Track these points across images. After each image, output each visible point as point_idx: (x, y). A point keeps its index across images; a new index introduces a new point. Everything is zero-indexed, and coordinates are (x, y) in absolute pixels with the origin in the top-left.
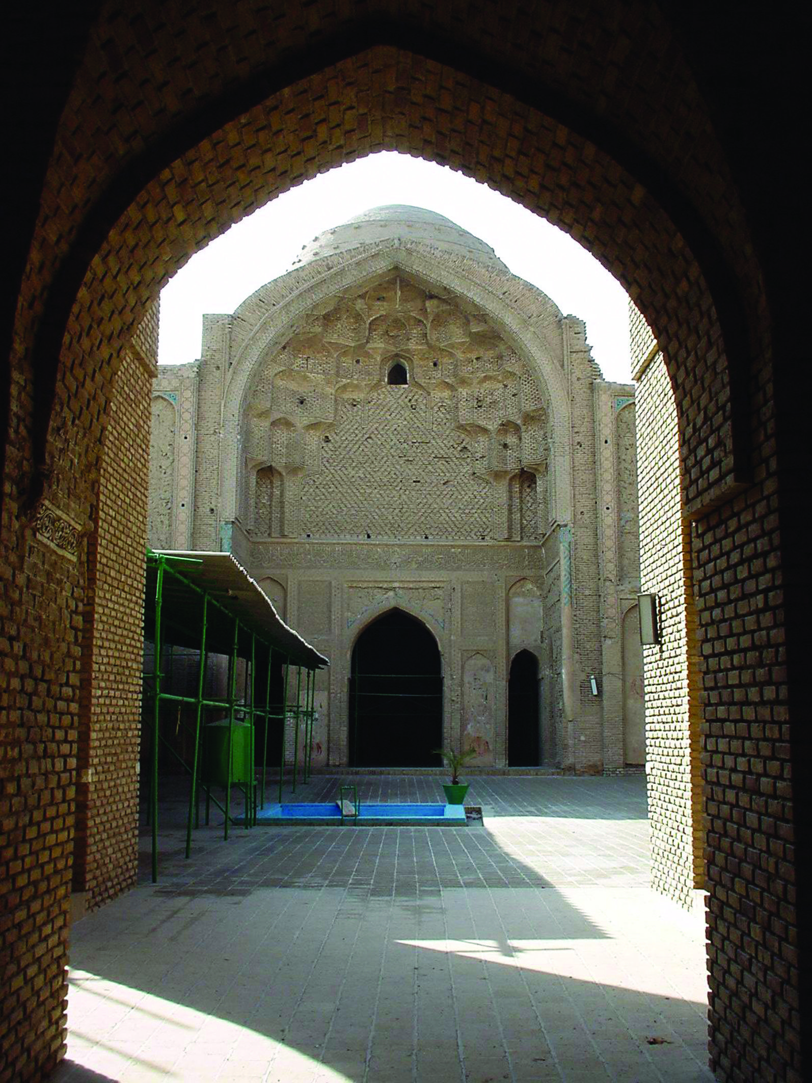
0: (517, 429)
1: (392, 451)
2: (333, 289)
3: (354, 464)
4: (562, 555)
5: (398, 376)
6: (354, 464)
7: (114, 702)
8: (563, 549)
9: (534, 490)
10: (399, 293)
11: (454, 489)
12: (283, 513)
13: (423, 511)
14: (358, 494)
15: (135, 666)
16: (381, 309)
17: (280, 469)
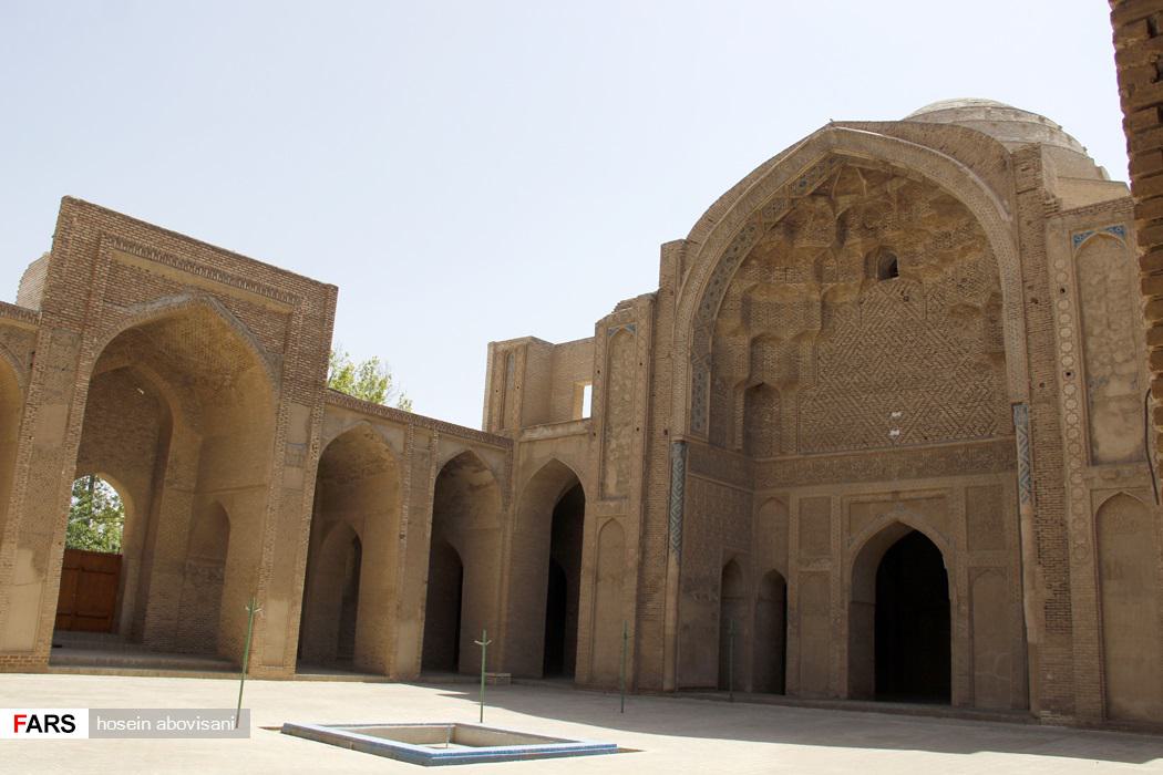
1: (886, 350)
3: (850, 370)
5: (892, 271)
6: (850, 370)
10: (865, 182)
11: (953, 382)
13: (921, 410)
14: (854, 402)
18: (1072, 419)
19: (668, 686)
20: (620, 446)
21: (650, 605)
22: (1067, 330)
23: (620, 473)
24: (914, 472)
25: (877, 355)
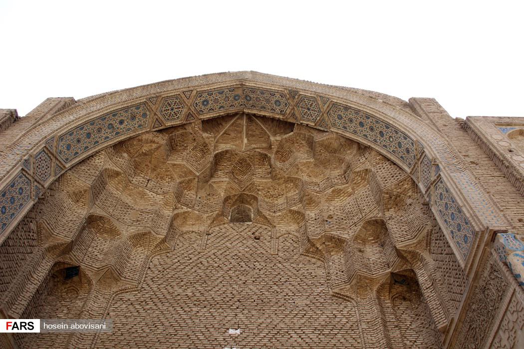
1: (231, 272)
6: (182, 283)
10: (245, 141)
17: (90, 274)
25: (219, 275)
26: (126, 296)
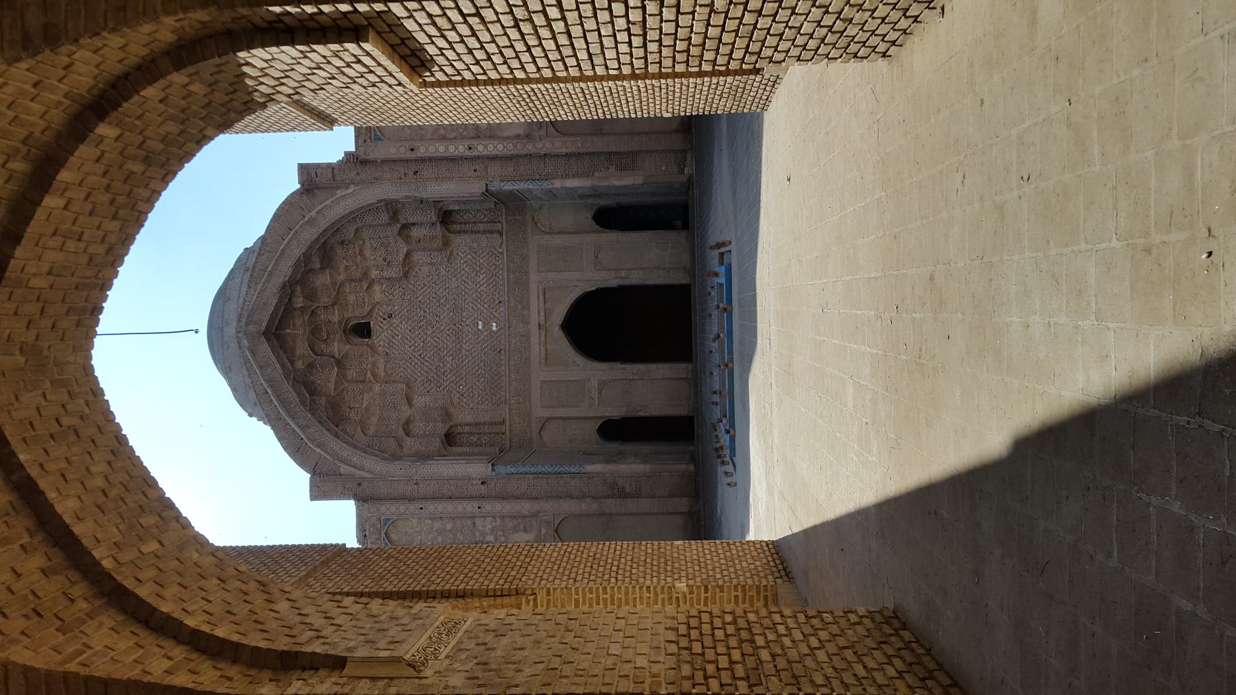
0: (406, 227)
2: (286, 387)
4: (511, 188)
5: (363, 330)
7: (622, 566)
8: (508, 187)
9: (457, 212)
12: (484, 424)
15: (594, 549)
16: (302, 348)
18: (500, 147)
19: (692, 467)
20: (493, 530)
21: (628, 489)
22: (441, 149)
23: (515, 529)
24: (525, 312)
26: (456, 400)
